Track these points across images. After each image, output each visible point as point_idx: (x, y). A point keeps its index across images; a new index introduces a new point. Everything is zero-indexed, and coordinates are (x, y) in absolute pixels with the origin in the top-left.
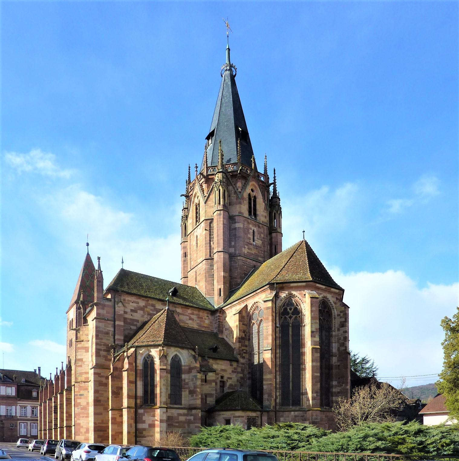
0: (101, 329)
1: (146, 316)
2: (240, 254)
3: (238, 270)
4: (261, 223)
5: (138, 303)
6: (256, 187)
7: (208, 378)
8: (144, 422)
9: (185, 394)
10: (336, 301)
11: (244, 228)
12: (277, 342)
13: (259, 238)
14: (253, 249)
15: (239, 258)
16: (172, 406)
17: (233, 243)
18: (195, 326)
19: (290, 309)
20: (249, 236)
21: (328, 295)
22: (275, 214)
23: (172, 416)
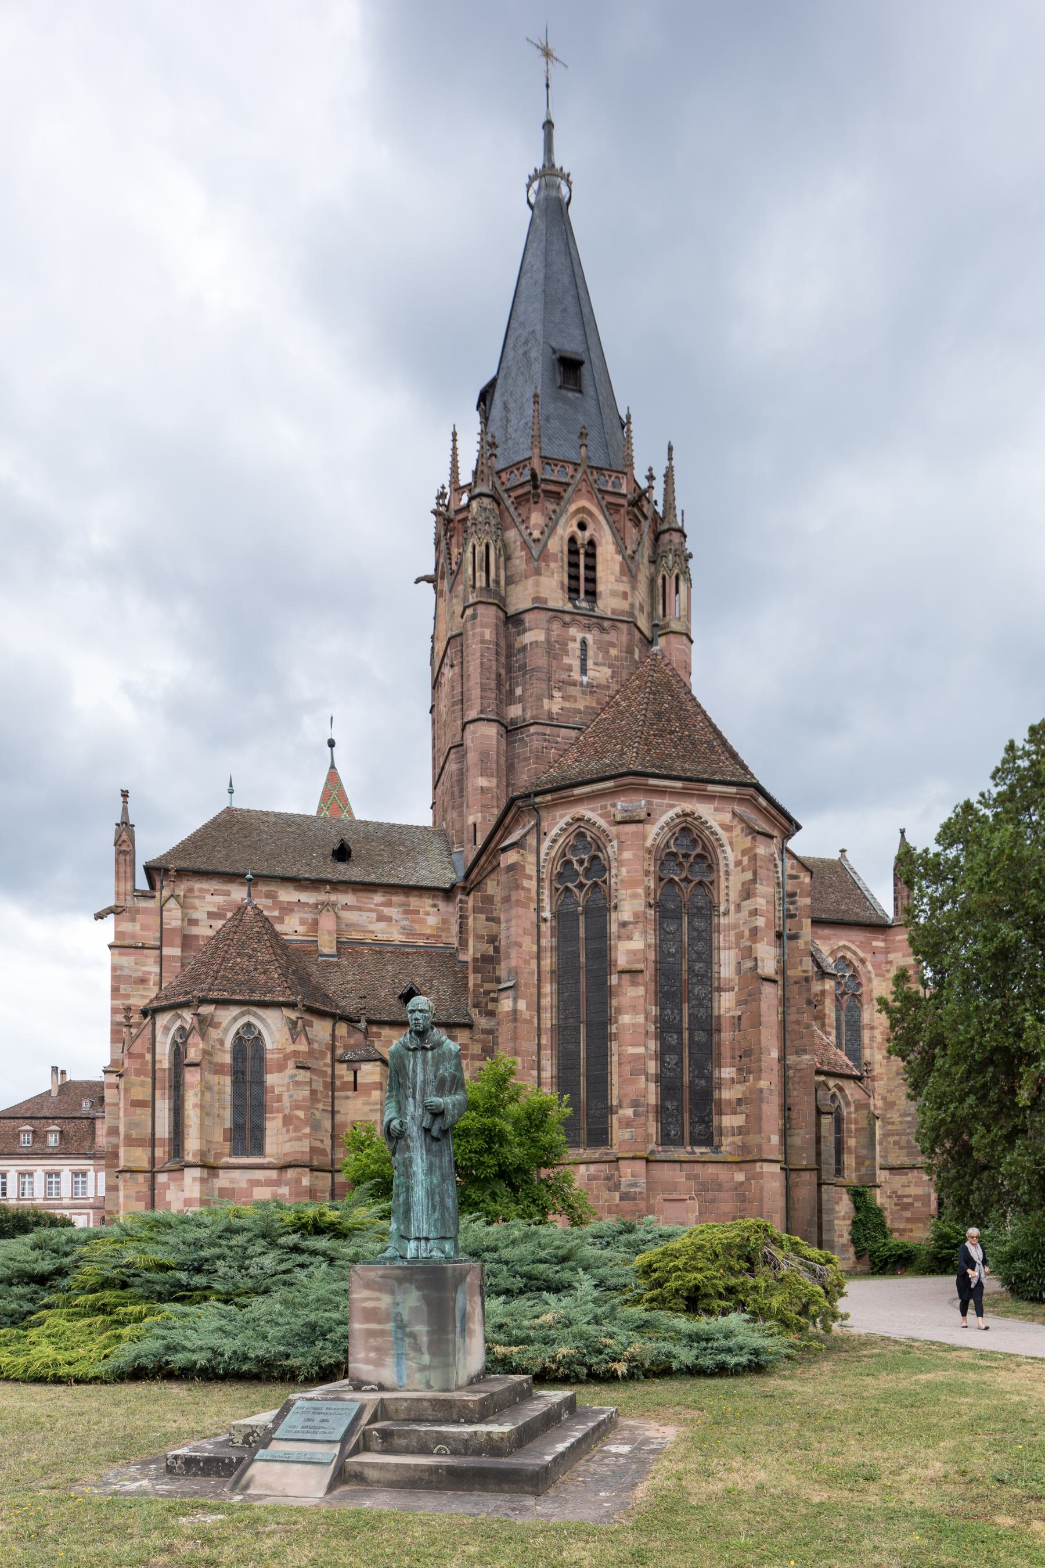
0: (126, 972)
3: (529, 764)
4: (609, 615)
6: (590, 514)
10: (731, 821)
12: (542, 963)
21: (698, 805)
22: (664, 578)
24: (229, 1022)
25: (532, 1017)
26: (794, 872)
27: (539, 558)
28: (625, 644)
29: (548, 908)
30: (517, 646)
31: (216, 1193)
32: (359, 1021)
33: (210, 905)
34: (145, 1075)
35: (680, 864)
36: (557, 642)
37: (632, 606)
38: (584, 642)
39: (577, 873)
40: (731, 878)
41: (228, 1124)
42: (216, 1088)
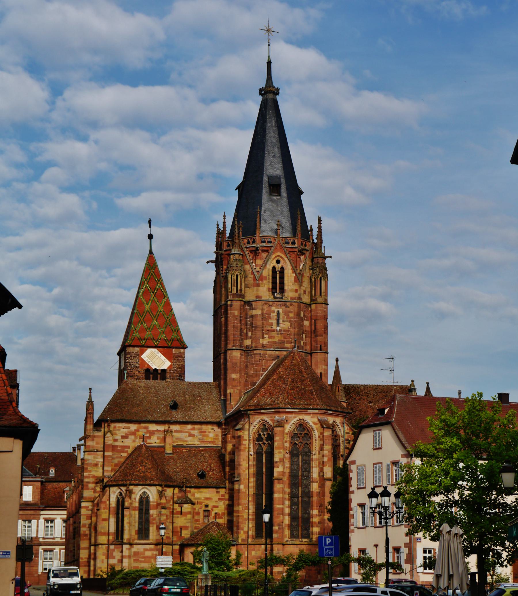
1: (137, 440)
2: (256, 347)
5: (129, 428)
7: (183, 511)
8: (114, 558)
9: (152, 529)
11: (262, 314)
13: (285, 319)
14: (276, 336)
15: (255, 352)
16: (138, 541)
17: (250, 334)
18: (197, 443)
19: (264, 435)
20: (270, 321)
22: (315, 278)
23: (138, 552)
24: (138, 491)
25: (246, 491)
26: (348, 431)
27: (258, 281)
28: (296, 312)
29: (252, 450)
30: (249, 314)
31: (132, 554)
32: (183, 487)
33: (126, 437)
34: (107, 509)
35: (299, 437)
36: (266, 314)
37: (300, 295)
38: (278, 313)
39: (262, 439)
40: (317, 442)
41: (137, 528)
42: (133, 516)
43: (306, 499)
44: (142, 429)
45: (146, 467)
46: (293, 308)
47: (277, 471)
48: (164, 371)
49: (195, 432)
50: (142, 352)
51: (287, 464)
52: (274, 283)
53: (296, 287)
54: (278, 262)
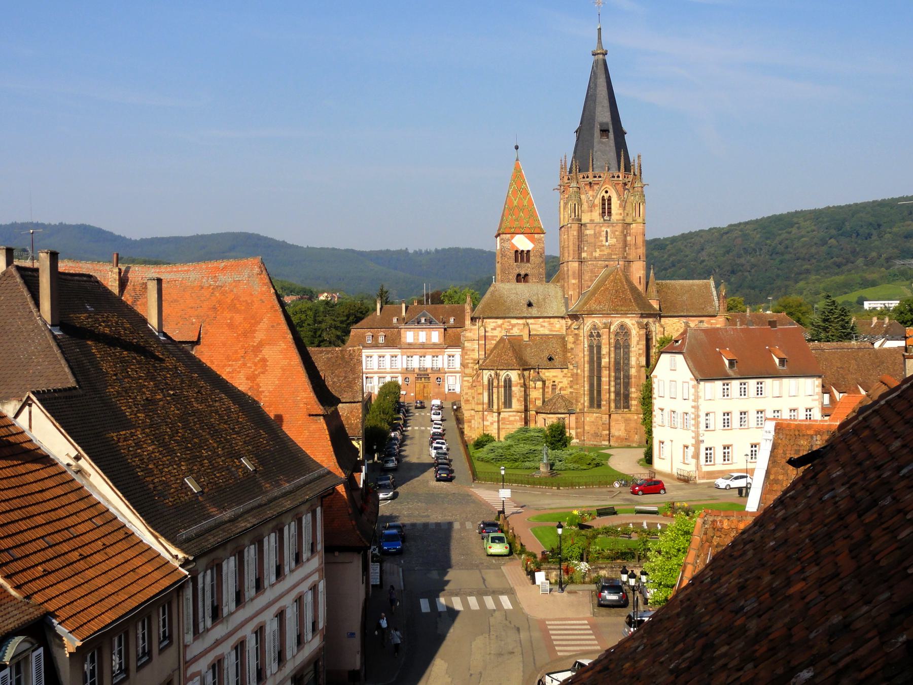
24: (503, 374)
43: (626, 380)
44: (506, 323)
45: (510, 356)
46: (619, 228)
47: (605, 361)
48: (528, 251)
49: (546, 324)
50: (512, 238)
51: (612, 355)
52: (604, 208)
53: (621, 211)
54: (607, 192)
